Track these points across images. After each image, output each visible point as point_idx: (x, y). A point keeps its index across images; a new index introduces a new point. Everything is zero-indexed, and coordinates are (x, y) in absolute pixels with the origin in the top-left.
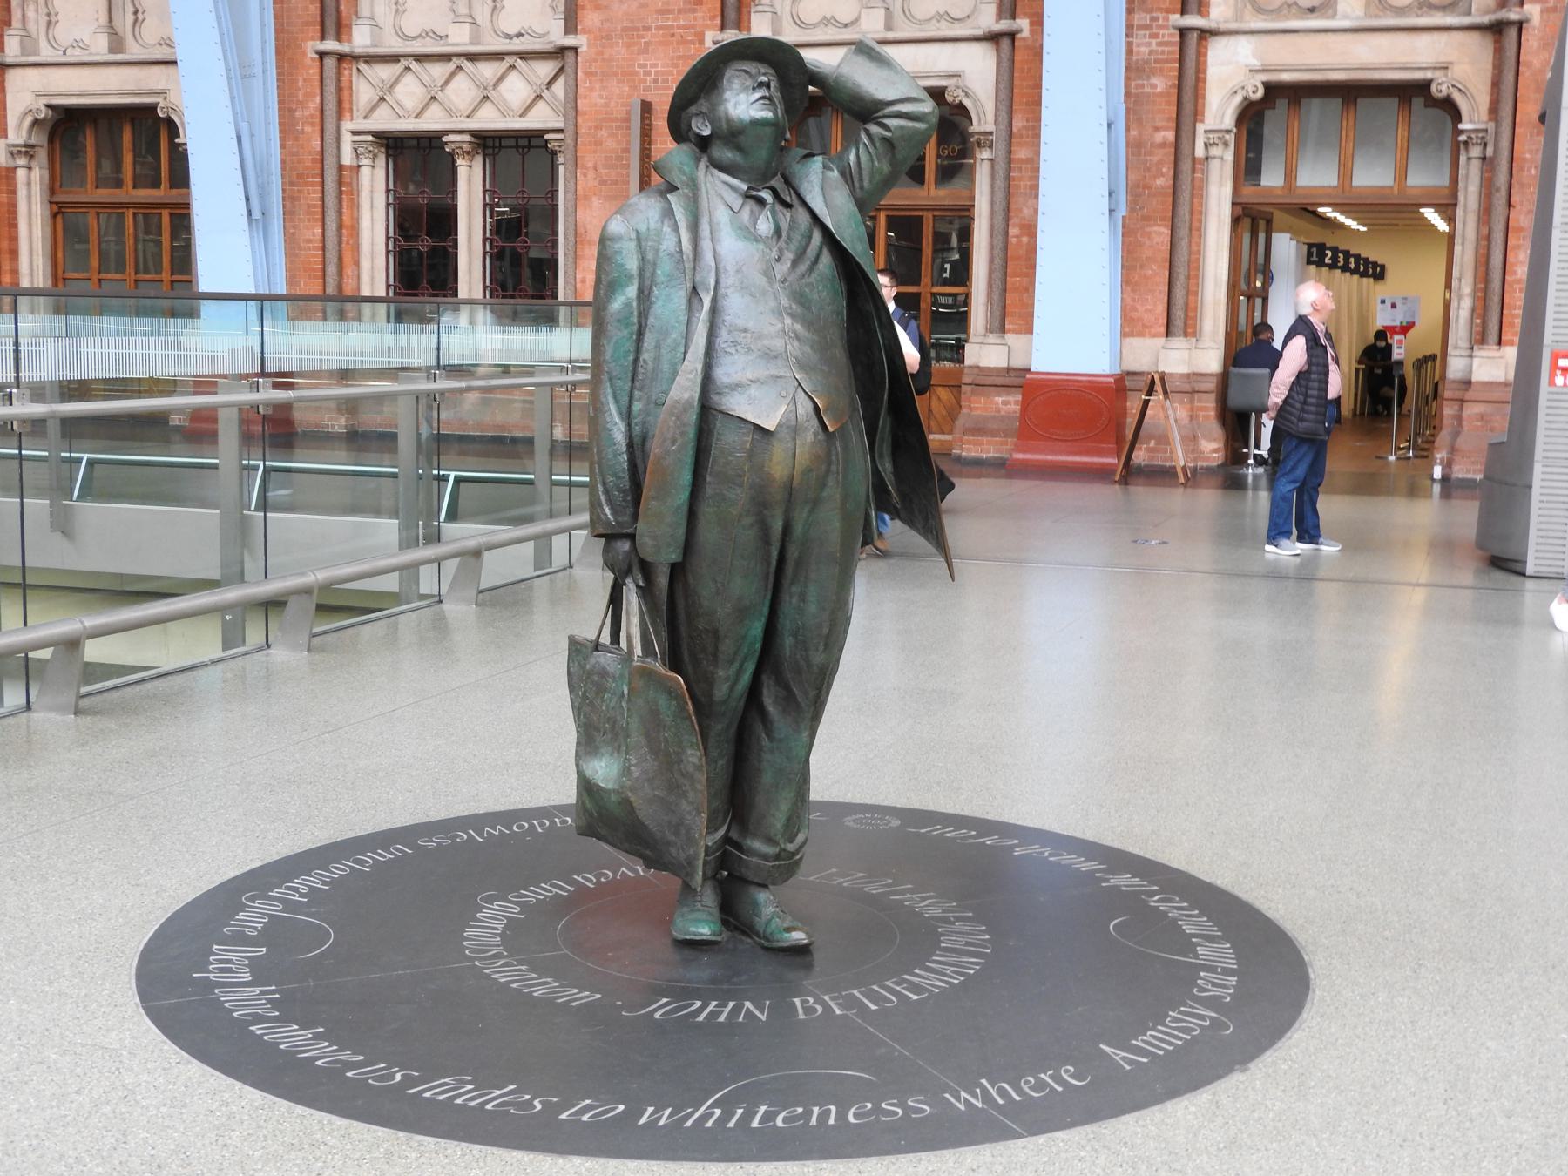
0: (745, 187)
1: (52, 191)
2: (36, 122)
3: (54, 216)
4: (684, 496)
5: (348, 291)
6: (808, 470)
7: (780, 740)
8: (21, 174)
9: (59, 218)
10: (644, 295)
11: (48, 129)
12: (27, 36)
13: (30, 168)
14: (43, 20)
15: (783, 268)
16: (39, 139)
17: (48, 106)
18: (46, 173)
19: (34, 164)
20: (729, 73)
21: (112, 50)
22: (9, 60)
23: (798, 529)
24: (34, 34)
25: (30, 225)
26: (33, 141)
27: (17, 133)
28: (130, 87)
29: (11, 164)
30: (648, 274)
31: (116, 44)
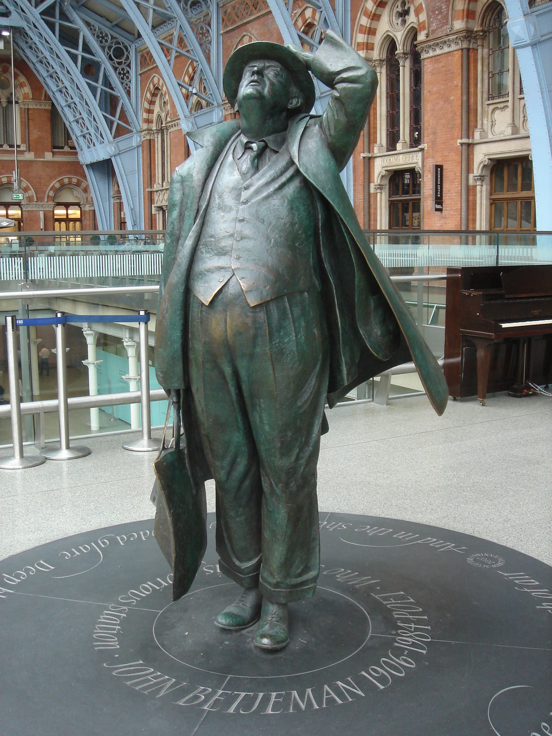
0: (245, 140)
1: (491, 194)
2: (484, 166)
3: (491, 204)
4: (178, 346)
5: (471, 229)
6: (238, 333)
7: (271, 512)
8: (478, 188)
9: (493, 205)
10: (181, 216)
11: (490, 169)
12: (483, 131)
13: (482, 185)
14: (490, 124)
15: (245, 195)
16: (487, 173)
17: (489, 159)
18: (489, 187)
19: (484, 183)
20: (247, 69)
21: (513, 134)
22: (475, 142)
23: (243, 373)
24: (486, 130)
25: (481, 209)
26: (482, 175)
27: (477, 170)
28: (519, 148)
29: (475, 184)
30: (184, 203)
31: (515, 129)
